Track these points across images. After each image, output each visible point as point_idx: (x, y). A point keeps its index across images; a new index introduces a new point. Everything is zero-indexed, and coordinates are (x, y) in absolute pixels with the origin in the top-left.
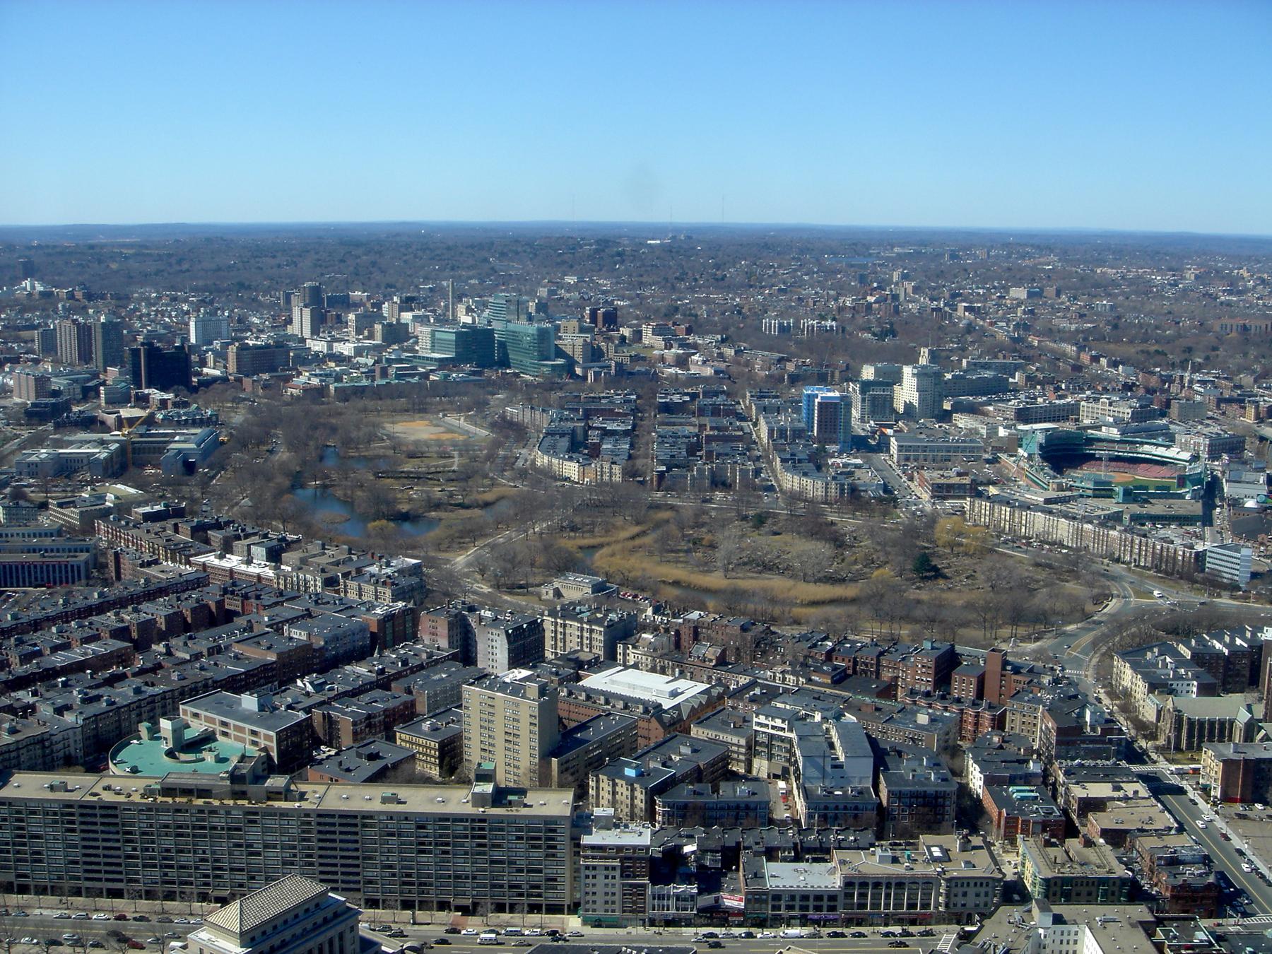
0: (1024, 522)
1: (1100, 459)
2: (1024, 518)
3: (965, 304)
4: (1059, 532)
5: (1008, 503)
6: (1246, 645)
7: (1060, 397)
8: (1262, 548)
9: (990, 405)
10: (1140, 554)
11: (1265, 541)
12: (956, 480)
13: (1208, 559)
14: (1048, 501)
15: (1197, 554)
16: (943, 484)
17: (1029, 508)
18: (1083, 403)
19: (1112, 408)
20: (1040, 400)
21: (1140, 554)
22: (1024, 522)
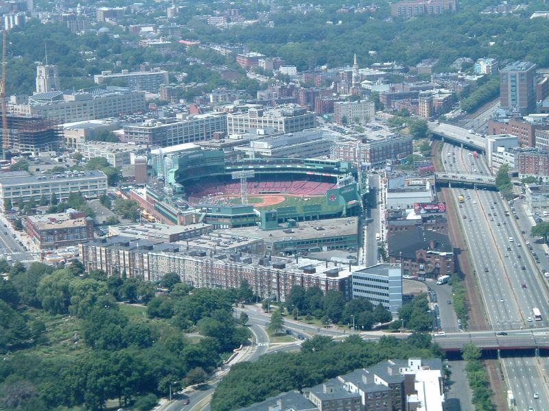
0: (146, 265)
1: (238, 181)
2: (145, 260)
3: (105, 9)
4: (187, 275)
5: (127, 245)
6: (386, 384)
7: (202, 111)
8: (422, 266)
9: (120, 128)
10: (278, 289)
11: (424, 257)
12: (70, 224)
13: (354, 287)
14: (174, 238)
15: (342, 282)
16: (53, 230)
17: (151, 248)
18: (229, 115)
19: (262, 119)
20: (179, 116)
21: (278, 289)
22: (146, 265)
